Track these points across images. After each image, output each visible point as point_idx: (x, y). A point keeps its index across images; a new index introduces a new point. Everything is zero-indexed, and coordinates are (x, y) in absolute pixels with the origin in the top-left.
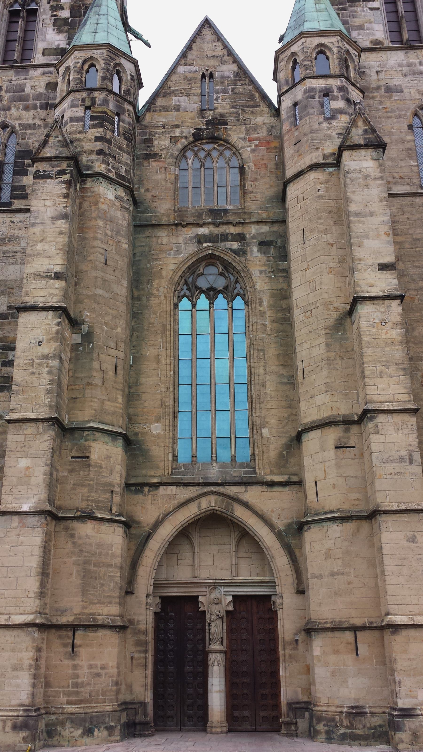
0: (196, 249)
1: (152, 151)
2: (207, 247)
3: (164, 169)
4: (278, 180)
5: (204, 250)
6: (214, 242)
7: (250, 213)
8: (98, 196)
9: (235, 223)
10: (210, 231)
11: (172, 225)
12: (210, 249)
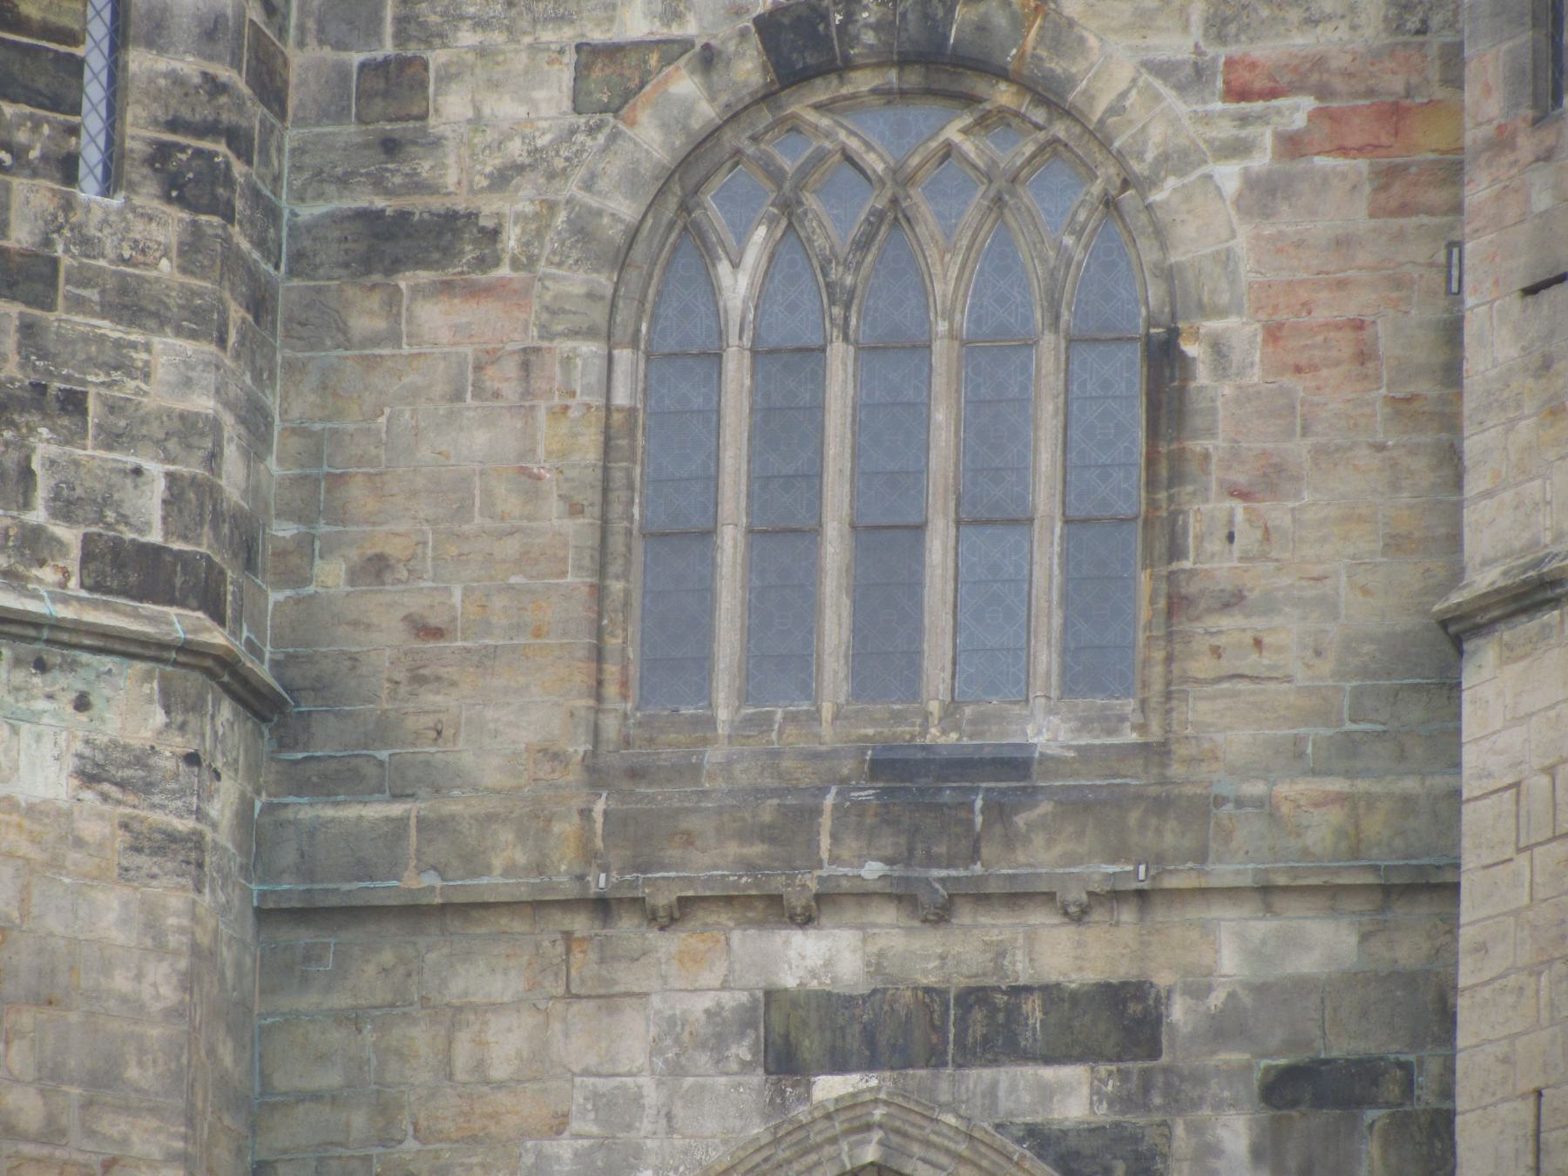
0: (757, 1129)
1: (417, 186)
2: (850, 1103)
3: (511, 367)
6: (901, 1058)
7: (1202, 809)
9: (1076, 894)
10: (876, 965)
11: (567, 905)
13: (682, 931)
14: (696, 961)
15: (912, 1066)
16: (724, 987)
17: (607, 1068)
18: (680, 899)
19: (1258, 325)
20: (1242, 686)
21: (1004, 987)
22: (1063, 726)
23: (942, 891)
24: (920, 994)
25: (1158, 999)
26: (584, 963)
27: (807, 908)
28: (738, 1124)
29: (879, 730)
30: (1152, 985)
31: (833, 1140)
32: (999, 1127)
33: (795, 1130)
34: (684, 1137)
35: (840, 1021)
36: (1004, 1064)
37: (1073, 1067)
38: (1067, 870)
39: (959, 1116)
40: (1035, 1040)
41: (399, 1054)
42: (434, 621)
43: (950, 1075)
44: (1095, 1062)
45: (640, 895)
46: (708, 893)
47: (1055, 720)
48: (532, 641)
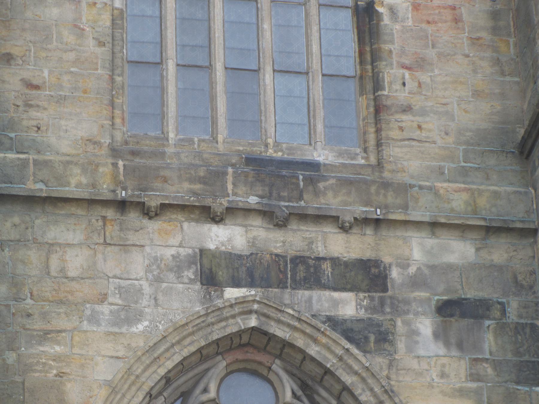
0: (198, 308)
2: (241, 301)
4: (503, 74)
5: (227, 313)
8: (380, 262)
9: (349, 218)
10: (252, 243)
12: (250, 312)
13: (160, 221)
14: (166, 234)
15: (271, 287)
16: (180, 246)
17: (125, 276)
18: (161, 204)
19: (409, 3)
20: (414, 143)
21: (313, 257)
22: (330, 154)
23: (286, 211)
24: (274, 257)
25: (385, 268)
26: (112, 230)
27: (222, 213)
28: (189, 305)
29: (245, 148)
30: (382, 262)
31: (233, 317)
32: (313, 316)
33: (215, 310)
34: (163, 309)
35: (236, 265)
36: (314, 289)
37: (347, 293)
38: (344, 208)
39: (294, 310)
40: (329, 280)
41: (23, 262)
42: (35, 82)
43: (289, 292)
44: (358, 291)
45: (143, 201)
46: (175, 203)
47: (326, 152)
48: (82, 95)
